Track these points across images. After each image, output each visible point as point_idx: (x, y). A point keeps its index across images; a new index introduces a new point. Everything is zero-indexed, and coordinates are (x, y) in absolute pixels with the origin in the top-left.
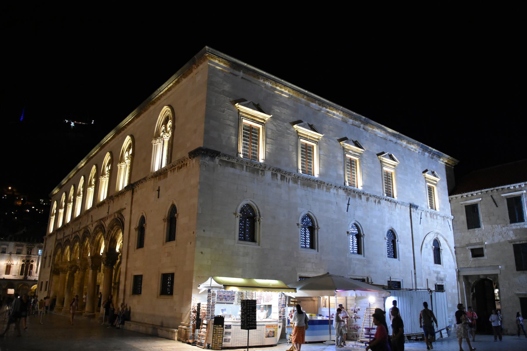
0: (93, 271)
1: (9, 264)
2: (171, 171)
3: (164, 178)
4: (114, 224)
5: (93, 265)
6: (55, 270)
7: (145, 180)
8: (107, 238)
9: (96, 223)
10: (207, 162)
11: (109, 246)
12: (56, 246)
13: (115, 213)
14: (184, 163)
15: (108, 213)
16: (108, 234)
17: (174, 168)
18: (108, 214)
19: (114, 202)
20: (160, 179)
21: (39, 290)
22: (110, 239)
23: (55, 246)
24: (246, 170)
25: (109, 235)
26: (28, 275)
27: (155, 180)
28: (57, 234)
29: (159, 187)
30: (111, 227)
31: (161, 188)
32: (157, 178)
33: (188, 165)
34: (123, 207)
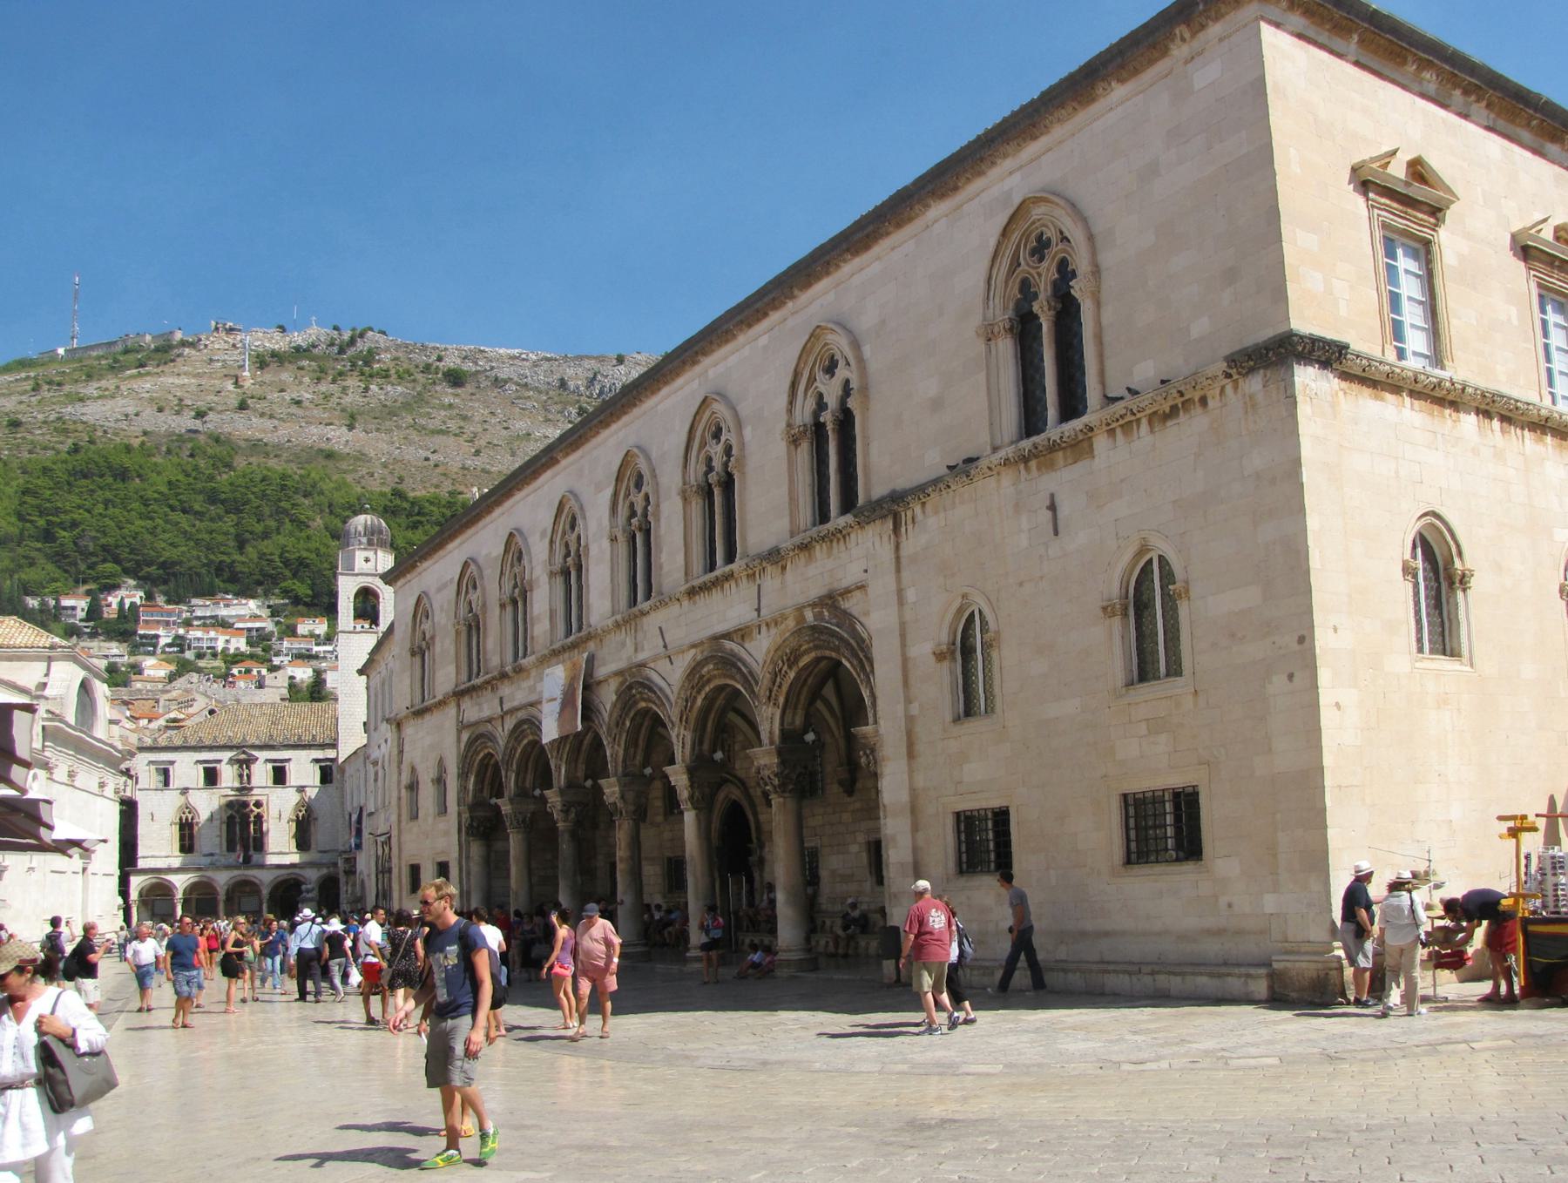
0: (697, 815)
1: (187, 819)
2: (1112, 432)
3: (1075, 462)
4: (801, 646)
5: (697, 794)
6: (475, 824)
7: (968, 476)
8: (769, 698)
9: (693, 651)
10: (1313, 385)
11: (782, 723)
12: (463, 746)
13: (800, 609)
14: (1186, 397)
15: (758, 610)
16: (774, 684)
17: (1133, 418)
18: (759, 616)
19: (784, 568)
20: (1051, 466)
21: (404, 893)
22: (781, 700)
23: (458, 747)
24: (1412, 405)
25: (780, 687)
26: (252, 849)
27: (1023, 471)
28: (458, 706)
29: (1052, 496)
30: (788, 660)
31: (1057, 500)
32: (1033, 464)
33: (1211, 403)
34: (848, 580)
